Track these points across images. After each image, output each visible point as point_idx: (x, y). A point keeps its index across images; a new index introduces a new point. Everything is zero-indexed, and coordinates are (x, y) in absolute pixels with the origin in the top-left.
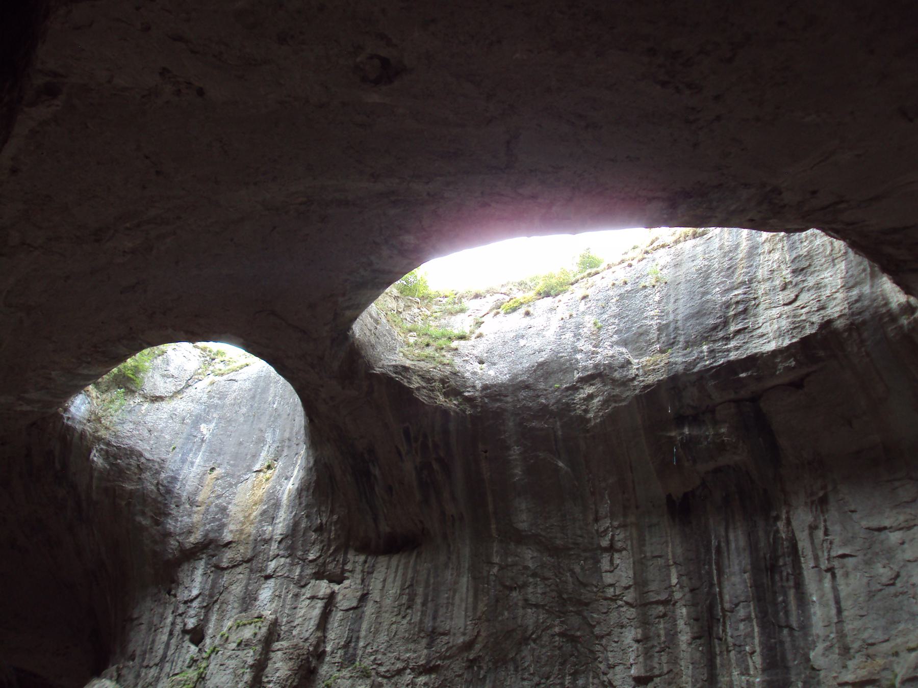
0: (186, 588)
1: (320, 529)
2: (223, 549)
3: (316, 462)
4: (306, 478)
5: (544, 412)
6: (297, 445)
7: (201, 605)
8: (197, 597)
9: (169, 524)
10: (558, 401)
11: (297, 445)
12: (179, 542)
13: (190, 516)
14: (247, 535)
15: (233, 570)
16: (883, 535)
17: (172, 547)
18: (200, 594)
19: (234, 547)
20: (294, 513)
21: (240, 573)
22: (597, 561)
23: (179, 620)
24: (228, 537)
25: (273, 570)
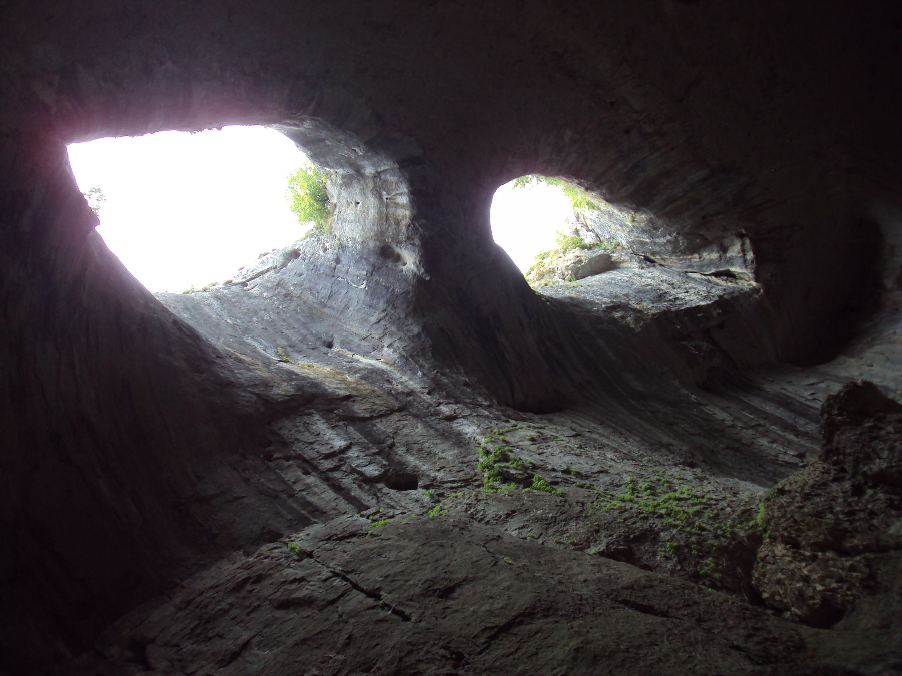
0: (312, 443)
1: (466, 384)
2: (345, 403)
3: (424, 328)
4: (413, 345)
5: (599, 320)
6: (313, 349)
7: (367, 452)
8: (348, 447)
9: (222, 372)
10: (606, 316)
11: (313, 349)
12: (257, 395)
13: (249, 370)
14: (368, 391)
15: (384, 420)
16: (815, 386)
17: (247, 398)
18: (351, 444)
19: (361, 400)
20: (420, 373)
21: (399, 420)
22: (702, 410)
23: (337, 475)
24: (343, 393)
25: (453, 412)
